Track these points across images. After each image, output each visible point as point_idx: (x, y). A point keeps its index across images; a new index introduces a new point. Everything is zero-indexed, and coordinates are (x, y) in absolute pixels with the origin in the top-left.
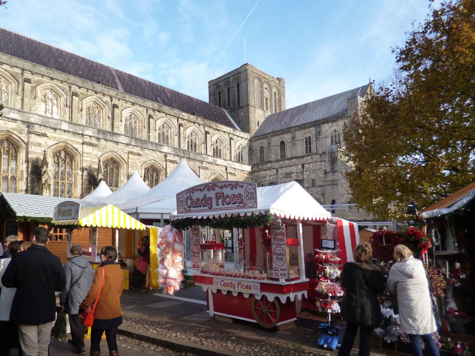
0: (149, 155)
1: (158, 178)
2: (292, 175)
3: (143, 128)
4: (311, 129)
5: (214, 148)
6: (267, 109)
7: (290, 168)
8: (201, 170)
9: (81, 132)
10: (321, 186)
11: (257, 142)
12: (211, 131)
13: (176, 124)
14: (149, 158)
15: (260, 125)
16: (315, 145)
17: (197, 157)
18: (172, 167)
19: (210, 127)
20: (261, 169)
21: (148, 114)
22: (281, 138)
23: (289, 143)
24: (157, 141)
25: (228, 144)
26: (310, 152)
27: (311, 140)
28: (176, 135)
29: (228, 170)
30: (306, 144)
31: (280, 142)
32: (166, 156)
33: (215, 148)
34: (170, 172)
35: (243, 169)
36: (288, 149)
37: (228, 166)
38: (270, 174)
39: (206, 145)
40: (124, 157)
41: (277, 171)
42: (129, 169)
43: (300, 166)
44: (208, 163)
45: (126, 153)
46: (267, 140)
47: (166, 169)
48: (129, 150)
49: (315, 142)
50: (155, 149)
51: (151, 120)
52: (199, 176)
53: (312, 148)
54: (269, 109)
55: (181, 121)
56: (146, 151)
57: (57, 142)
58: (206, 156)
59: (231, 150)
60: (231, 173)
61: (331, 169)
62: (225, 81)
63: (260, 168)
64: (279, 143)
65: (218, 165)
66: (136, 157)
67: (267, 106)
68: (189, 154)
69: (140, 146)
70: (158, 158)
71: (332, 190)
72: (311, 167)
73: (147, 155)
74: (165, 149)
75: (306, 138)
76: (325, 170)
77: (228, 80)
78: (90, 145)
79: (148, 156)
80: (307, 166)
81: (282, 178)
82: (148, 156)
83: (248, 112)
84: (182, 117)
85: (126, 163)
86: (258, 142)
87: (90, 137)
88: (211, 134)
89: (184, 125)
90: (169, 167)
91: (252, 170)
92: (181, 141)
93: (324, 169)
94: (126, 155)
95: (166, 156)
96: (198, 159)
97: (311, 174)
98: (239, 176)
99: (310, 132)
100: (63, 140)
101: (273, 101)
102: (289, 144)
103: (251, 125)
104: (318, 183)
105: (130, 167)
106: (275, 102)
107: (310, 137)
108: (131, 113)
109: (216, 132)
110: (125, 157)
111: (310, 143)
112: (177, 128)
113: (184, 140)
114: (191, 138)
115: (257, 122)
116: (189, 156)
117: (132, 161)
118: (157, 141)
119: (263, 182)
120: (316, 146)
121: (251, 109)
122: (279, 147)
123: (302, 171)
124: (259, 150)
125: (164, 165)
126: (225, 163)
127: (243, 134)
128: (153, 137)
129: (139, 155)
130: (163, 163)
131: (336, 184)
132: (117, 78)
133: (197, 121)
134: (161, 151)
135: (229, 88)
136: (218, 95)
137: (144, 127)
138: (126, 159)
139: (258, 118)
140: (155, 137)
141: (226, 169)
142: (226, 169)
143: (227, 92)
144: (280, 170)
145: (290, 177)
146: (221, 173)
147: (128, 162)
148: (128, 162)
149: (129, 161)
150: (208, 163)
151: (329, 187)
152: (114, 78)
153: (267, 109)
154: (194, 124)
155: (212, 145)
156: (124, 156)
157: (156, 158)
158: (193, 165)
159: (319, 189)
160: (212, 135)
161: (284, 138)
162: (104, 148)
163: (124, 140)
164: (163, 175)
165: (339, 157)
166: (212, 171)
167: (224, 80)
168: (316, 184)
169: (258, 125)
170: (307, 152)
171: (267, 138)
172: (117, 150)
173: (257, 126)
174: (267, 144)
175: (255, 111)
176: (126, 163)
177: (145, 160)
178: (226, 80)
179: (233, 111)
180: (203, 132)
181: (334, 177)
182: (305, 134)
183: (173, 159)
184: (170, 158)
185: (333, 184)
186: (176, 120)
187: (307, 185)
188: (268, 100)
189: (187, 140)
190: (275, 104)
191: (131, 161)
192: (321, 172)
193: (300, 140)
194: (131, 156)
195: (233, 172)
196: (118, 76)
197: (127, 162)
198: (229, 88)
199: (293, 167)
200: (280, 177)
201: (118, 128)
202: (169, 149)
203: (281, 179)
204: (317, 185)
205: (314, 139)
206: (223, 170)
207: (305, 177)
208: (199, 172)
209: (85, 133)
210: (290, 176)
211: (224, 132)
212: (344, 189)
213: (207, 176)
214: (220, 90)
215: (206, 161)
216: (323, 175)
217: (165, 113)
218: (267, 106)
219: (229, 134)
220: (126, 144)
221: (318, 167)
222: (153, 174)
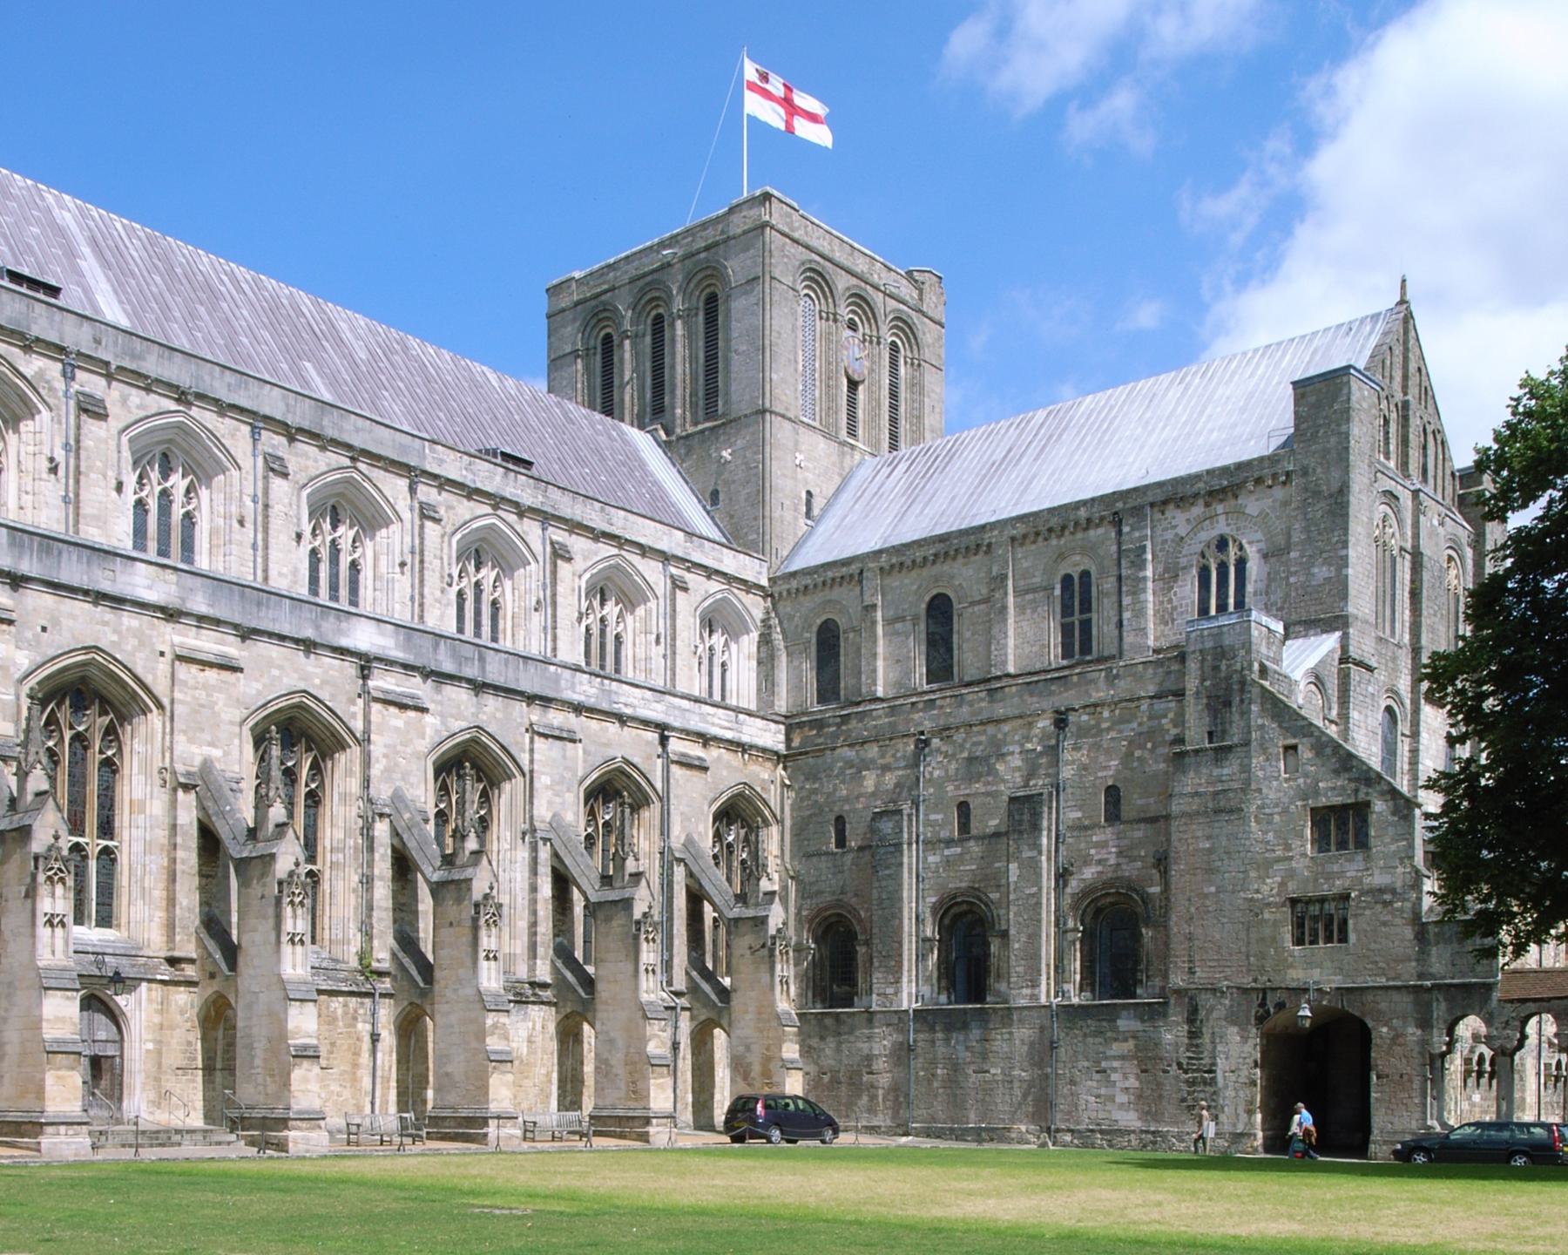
0: (280, 667)
1: (322, 785)
2: (1000, 767)
3: (236, 525)
4: (1093, 533)
5: (588, 629)
6: (852, 432)
7: (991, 729)
8: (539, 743)
10: (1153, 820)
11: (801, 598)
12: (578, 544)
13: (403, 503)
14: (280, 678)
15: (816, 512)
16: (1113, 613)
17: (522, 675)
18: (397, 729)
19: (576, 527)
20: (835, 736)
21: (260, 447)
22: (936, 579)
23: (979, 602)
24: (303, 591)
25: (662, 610)
26: (1086, 648)
27: (1094, 589)
28: (403, 564)
29: (676, 745)
30: (1067, 610)
31: (927, 598)
32: (365, 673)
33: (595, 631)
34: (385, 756)
35: (745, 739)
36: (968, 634)
37: (672, 721)
38: (881, 761)
39: (554, 616)
40: (148, 680)
41: (923, 744)
42: (180, 738)
43: (1044, 723)
44: (578, 709)
45: (162, 654)
46: (858, 589)
47: (365, 741)
48: (177, 639)
49: (1114, 598)
50: (308, 633)
51: (277, 483)
52: (532, 772)
53: (1094, 631)
54: (860, 432)
55: (427, 493)
56: (265, 648)
58: (567, 674)
59: (674, 639)
60: (686, 763)
61: (1210, 734)
62: (640, 283)
63: (832, 729)
64: (924, 606)
65: (622, 719)
66: (212, 675)
67: (852, 416)
68: (482, 659)
69: (237, 620)
70: (324, 682)
71: (1209, 838)
72: (1105, 725)
73: (270, 663)
74: (364, 637)
75: (1067, 581)
76: (1180, 740)
77: (655, 276)
79: (275, 672)
80: (1085, 718)
81: (948, 778)
82: (275, 672)
83: (759, 445)
84: (436, 470)
85: (160, 706)
86: (808, 602)
88: (578, 558)
89: (442, 511)
90: (380, 733)
91: (788, 740)
92: (426, 591)
93: (1174, 731)
94: (163, 666)
95: (365, 673)
96: (525, 686)
97: (1102, 758)
98: (725, 773)
99: (1089, 550)
101: (885, 392)
102: (976, 608)
103: (777, 514)
104: (1134, 802)
105: (185, 732)
106: (894, 395)
107: (1085, 575)
108: (170, 441)
109: (606, 550)
110: (157, 675)
111: (1086, 606)
112: (408, 525)
113: (443, 591)
114: (474, 580)
115: (804, 495)
116: (483, 669)
117: (194, 697)
118: (303, 591)
119: (846, 800)
120: (1115, 619)
121: (779, 431)
122: (923, 626)
123: (1053, 742)
124: (814, 640)
125: (354, 716)
126: (656, 710)
127: (731, 562)
128: (285, 570)
130: (353, 709)
131: (1231, 811)
132: (86, 250)
133: (509, 491)
134: (344, 642)
135: (659, 320)
136: (599, 357)
137: (241, 523)
138: (161, 689)
139: (810, 476)
140: (295, 572)
141: (664, 741)
142: (664, 741)
143: (648, 339)
144: (936, 742)
145: (988, 774)
146: (635, 760)
147: (172, 702)
148: (172, 702)
149: (177, 695)
150: (578, 709)
151: (1198, 829)
152: (72, 254)
153: (852, 432)
154: (496, 507)
155: (580, 620)
156: (153, 670)
157: (317, 681)
158: (499, 715)
159: (1139, 833)
160: (579, 563)
161: (952, 577)
162: (44, 629)
163: (150, 588)
164: (349, 773)
165: (1255, 676)
166: (592, 748)
167: (632, 281)
168: (1127, 811)
169: (808, 515)
170: (1067, 652)
171: (860, 582)
172: (115, 638)
173: (802, 521)
174: (855, 610)
175: (796, 443)
176: (160, 706)
177: (259, 693)
178: (649, 278)
179: (680, 438)
180: (537, 546)
181: (1225, 771)
182: (1061, 557)
183: (399, 689)
184: (382, 681)
185: (1217, 811)
186: (403, 484)
187: (1079, 814)
188: (861, 388)
189: (455, 588)
190: (894, 408)
191: (188, 699)
192: (1154, 747)
193: (1034, 590)
194: (183, 671)
195: (695, 750)
196: (94, 243)
197: (166, 702)
198: (659, 320)
199: (1006, 728)
200: (936, 773)
201: (101, 521)
202: (382, 634)
203: (939, 784)
204: (1134, 815)
205: (1109, 584)
206: (648, 743)
207: (1067, 772)
208: (532, 751)
210: (992, 771)
211: (644, 551)
212: (1270, 836)
213: (568, 775)
214: (608, 330)
215: (568, 695)
216: (1162, 766)
217: (349, 447)
218: (852, 416)
219: (665, 558)
220: (162, 609)
221: (1140, 724)
222: (298, 764)
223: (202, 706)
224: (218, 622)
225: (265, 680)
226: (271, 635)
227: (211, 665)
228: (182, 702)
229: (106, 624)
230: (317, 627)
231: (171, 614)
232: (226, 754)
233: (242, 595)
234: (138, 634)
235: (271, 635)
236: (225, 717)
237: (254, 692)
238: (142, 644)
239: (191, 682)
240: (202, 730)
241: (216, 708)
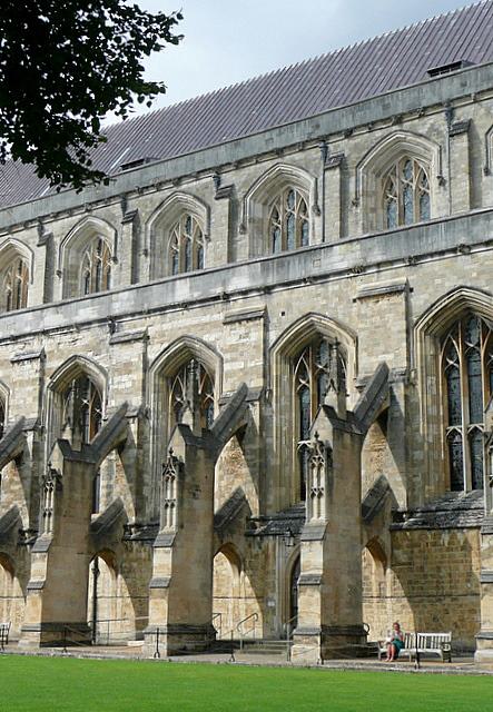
0: (443, 276)
9: (218, 291)
14: (442, 285)
40: (346, 321)
57: (166, 345)
66: (384, 303)
78: (240, 321)
79: (438, 281)
82: (438, 281)
87: (244, 293)
100: (180, 334)
105: (366, 350)
129: (393, 292)
156: (349, 314)
157: (474, 275)
162: (283, 314)
172: (324, 302)
209: (230, 289)
220: (349, 271)
223: (379, 327)
224: (391, 262)
225: (431, 290)
226: (432, 255)
227: (382, 295)
228: (363, 329)
229: (319, 295)
230: (469, 233)
231: (360, 270)
232: (396, 356)
233: (407, 236)
234: (340, 296)
235: (432, 255)
236: (394, 329)
237: (422, 302)
238: (341, 299)
239: (370, 313)
240: (378, 344)
241: (388, 326)
